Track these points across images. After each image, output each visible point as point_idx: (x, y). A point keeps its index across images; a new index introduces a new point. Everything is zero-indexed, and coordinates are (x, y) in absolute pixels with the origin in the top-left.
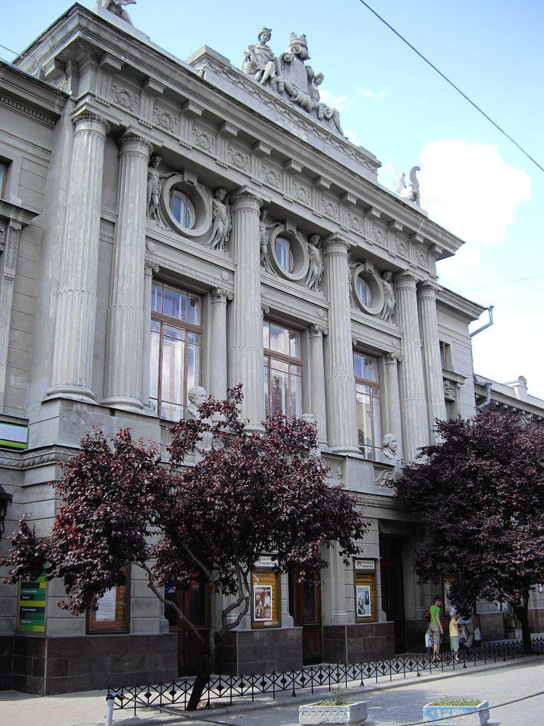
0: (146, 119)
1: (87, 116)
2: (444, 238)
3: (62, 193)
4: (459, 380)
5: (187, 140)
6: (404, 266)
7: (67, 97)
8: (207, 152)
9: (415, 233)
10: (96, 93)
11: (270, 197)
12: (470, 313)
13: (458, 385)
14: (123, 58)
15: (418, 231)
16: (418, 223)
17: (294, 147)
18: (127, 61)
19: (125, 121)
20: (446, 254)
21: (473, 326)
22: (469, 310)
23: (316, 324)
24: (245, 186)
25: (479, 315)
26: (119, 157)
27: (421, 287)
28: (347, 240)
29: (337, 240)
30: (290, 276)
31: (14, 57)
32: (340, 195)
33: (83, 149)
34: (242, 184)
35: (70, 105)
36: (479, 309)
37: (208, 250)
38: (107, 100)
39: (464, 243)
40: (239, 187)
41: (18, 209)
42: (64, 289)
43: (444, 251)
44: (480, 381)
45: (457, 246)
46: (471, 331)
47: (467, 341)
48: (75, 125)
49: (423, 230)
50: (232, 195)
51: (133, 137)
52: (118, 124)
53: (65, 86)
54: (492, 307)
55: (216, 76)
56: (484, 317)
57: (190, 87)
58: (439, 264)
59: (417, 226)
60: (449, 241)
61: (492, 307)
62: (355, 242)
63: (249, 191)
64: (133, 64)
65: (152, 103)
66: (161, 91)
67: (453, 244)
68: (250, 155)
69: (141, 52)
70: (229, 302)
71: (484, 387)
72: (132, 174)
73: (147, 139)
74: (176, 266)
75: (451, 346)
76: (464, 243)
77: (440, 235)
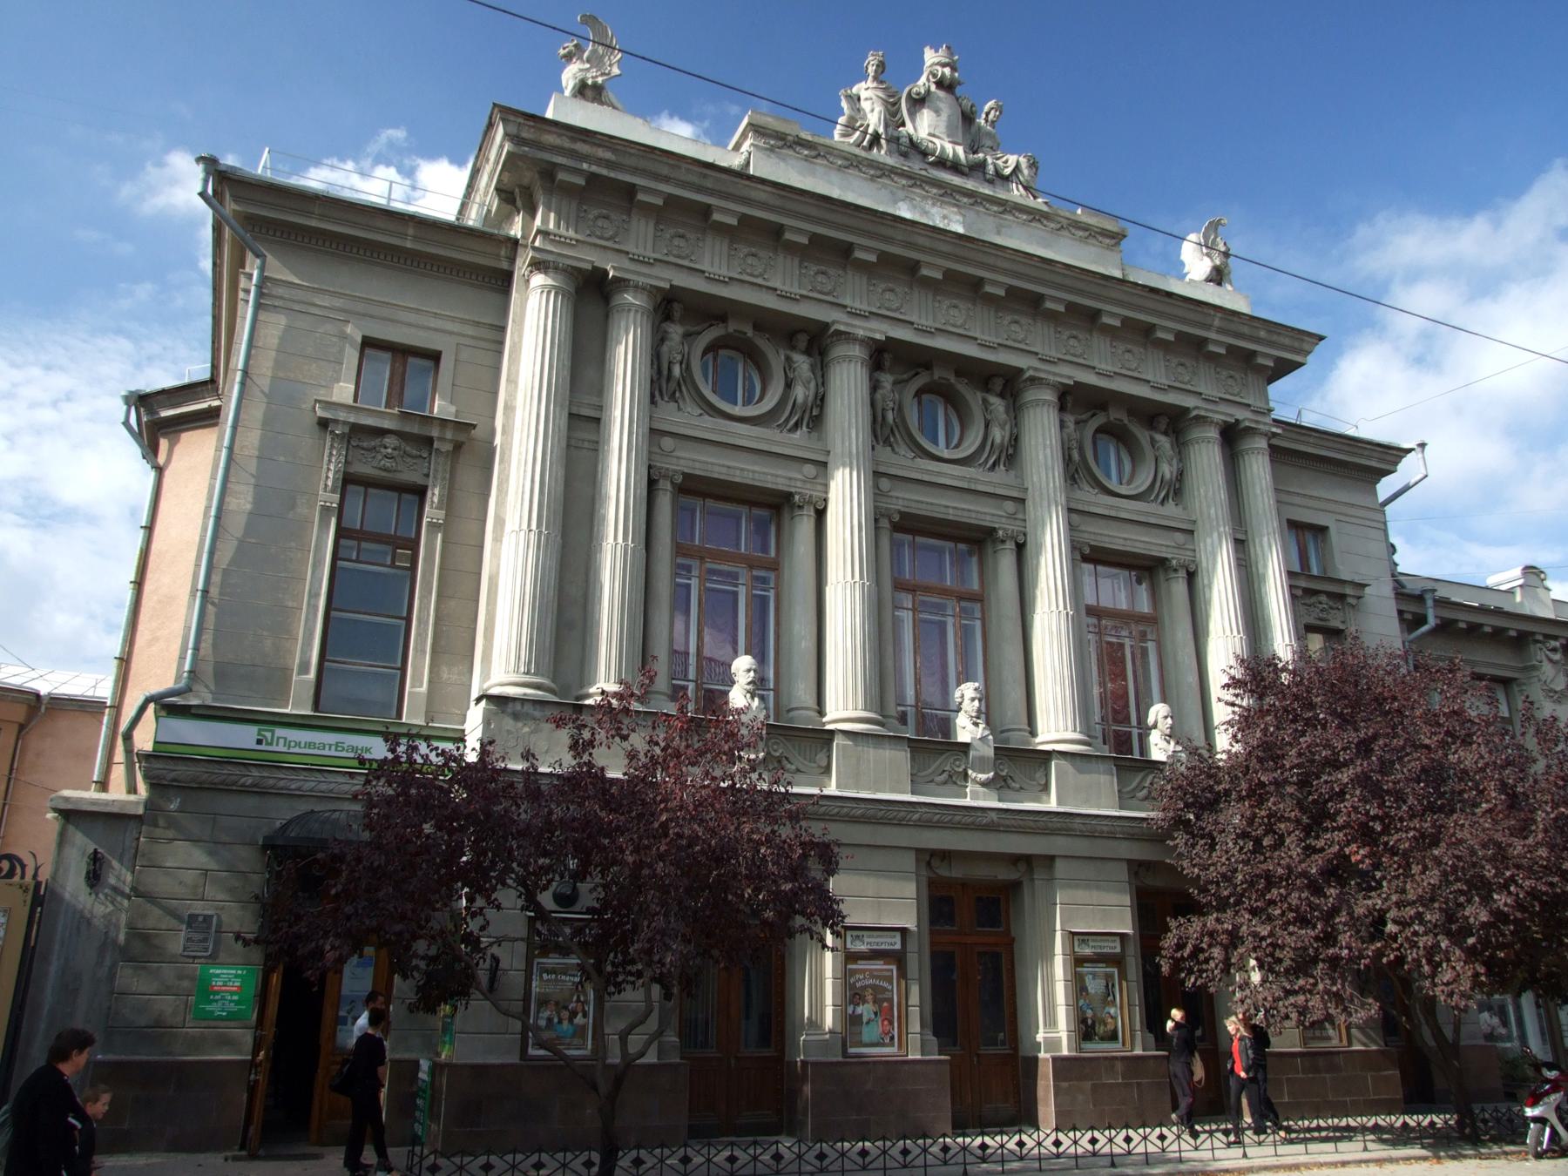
0: (638, 256)
2: (1275, 338)
4: (1348, 591)
5: (713, 269)
9: (1205, 341)
11: (880, 331)
12: (1374, 464)
13: (1350, 600)
14: (585, 166)
15: (1213, 335)
18: (594, 169)
20: (1284, 368)
21: (1385, 487)
22: (1369, 457)
24: (834, 322)
25: (1396, 463)
26: (607, 317)
27: (1232, 436)
28: (1051, 377)
29: (1033, 380)
30: (1123, 490)
34: (829, 320)
37: (785, 437)
39: (1321, 338)
40: (825, 326)
41: (444, 422)
43: (1278, 360)
44: (1413, 588)
45: (1306, 347)
46: (1381, 498)
47: (1378, 517)
49: (1221, 331)
50: (816, 341)
54: (1422, 445)
57: (709, 185)
58: (1277, 389)
59: (1208, 327)
60: (1287, 341)
61: (1422, 445)
63: (842, 328)
64: (604, 172)
67: (1296, 344)
68: (844, 268)
69: (614, 151)
71: (1420, 598)
73: (642, 280)
74: (717, 469)
75: (1333, 532)
76: (1321, 338)
77: (1262, 334)
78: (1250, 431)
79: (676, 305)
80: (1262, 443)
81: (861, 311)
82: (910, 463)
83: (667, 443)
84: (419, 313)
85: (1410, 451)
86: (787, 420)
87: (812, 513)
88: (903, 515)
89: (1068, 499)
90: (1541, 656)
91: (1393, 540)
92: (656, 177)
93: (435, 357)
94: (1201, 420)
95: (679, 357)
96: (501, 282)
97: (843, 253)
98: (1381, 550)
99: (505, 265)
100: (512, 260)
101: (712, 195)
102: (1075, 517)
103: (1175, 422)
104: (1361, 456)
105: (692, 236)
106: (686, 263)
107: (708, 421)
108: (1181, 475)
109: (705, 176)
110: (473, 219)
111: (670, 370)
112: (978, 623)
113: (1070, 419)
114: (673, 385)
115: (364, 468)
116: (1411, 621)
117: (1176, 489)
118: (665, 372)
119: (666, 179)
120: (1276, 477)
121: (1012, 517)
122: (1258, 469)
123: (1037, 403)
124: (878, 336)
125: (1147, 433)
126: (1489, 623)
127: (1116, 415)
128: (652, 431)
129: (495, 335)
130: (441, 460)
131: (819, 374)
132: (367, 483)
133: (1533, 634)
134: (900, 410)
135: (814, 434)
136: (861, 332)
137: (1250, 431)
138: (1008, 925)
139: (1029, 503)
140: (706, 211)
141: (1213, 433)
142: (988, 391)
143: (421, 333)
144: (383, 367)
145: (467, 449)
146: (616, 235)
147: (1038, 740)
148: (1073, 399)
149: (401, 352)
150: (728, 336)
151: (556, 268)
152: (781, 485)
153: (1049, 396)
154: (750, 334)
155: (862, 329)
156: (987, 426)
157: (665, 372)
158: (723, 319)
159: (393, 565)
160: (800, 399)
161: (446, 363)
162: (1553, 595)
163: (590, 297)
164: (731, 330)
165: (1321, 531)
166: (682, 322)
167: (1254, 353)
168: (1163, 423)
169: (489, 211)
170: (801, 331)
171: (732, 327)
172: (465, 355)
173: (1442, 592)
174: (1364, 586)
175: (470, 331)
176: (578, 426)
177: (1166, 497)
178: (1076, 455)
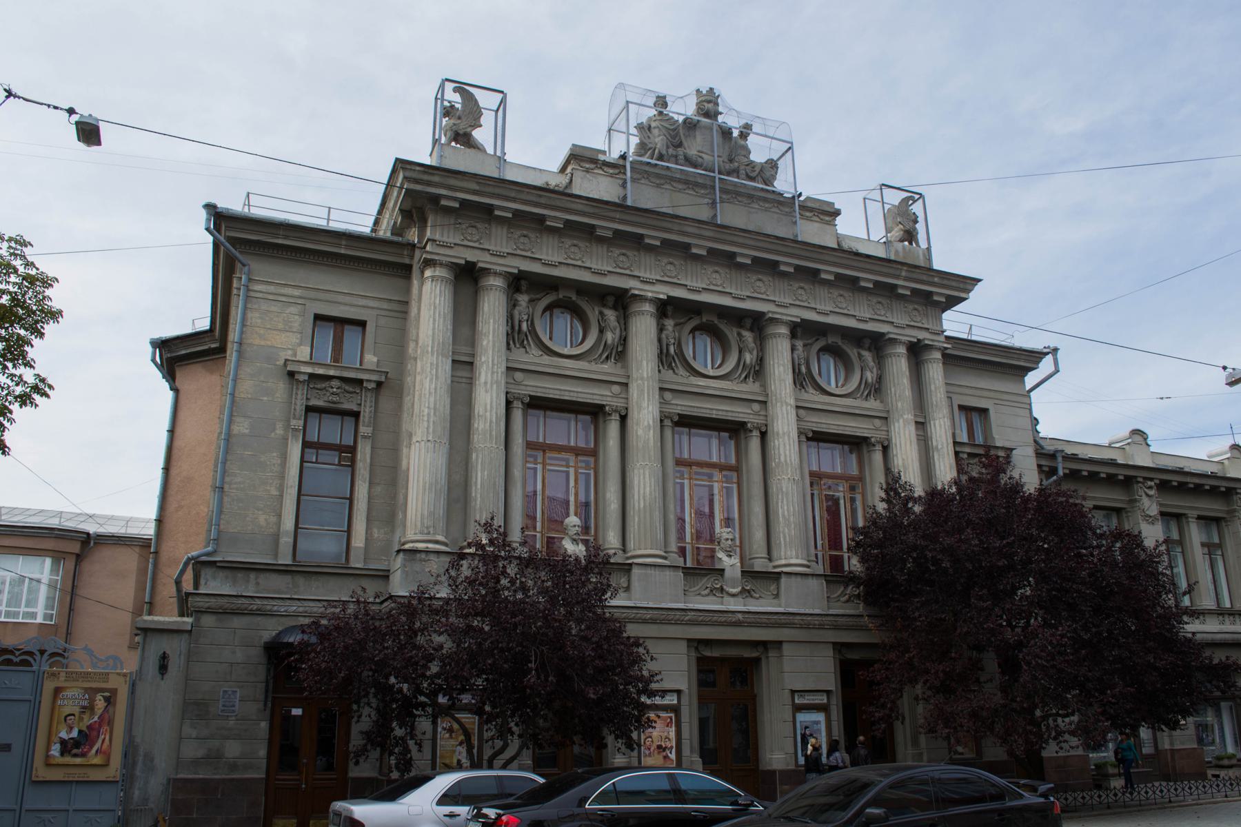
1: (428, 263)
3: (412, 345)
6: (883, 328)
7: (414, 246)
8: (579, 263)
10: (437, 237)
11: (663, 292)
12: (1022, 364)
16: (897, 273)
17: (690, 230)
19: (471, 256)
20: (953, 302)
21: (1031, 379)
22: (1019, 359)
25: (1038, 362)
29: (772, 319)
31: (370, 221)
32: (769, 268)
33: (431, 299)
35: (417, 253)
36: (1034, 357)
38: (451, 240)
42: (414, 440)
43: (948, 297)
44: (1050, 448)
47: (1025, 400)
48: (422, 273)
50: (621, 301)
51: (486, 272)
52: (463, 262)
53: (413, 236)
54: (1055, 350)
56: (1046, 365)
58: (947, 315)
65: (505, 230)
66: (510, 215)
72: (486, 309)
73: (498, 268)
75: (992, 413)
78: (929, 348)
79: (523, 282)
80: (938, 355)
81: (651, 280)
84: (350, 294)
85: (1047, 354)
89: (797, 400)
90: (1141, 492)
91: (1035, 414)
92: (507, 198)
93: (362, 324)
94: (893, 341)
96: (405, 271)
97: (636, 242)
98: (1027, 424)
99: (407, 261)
100: (412, 257)
102: (802, 412)
103: (877, 343)
104: (1012, 358)
105: (532, 235)
108: (880, 379)
109: (540, 196)
110: (384, 232)
112: (735, 486)
113: (799, 344)
114: (523, 336)
115: (313, 402)
116: (1047, 471)
119: (514, 200)
120: (946, 374)
122: (935, 372)
124: (661, 296)
125: (855, 351)
126: (1104, 471)
127: (831, 340)
128: (508, 368)
129: (402, 310)
130: (369, 394)
132: (320, 411)
133: (1136, 477)
134: (679, 345)
135: (619, 365)
136: (650, 294)
138: (752, 685)
141: (902, 350)
142: (742, 327)
143: (353, 309)
144: (328, 334)
145: (388, 386)
148: (801, 330)
149: (340, 323)
151: (441, 264)
153: (784, 330)
159: (339, 464)
161: (370, 328)
162: (1152, 449)
163: (467, 277)
165: (984, 412)
167: (931, 293)
168: (867, 342)
169: (395, 223)
172: (382, 321)
173: (1070, 450)
174: (1012, 450)
175: (385, 305)
176: (464, 365)
177: (869, 394)
178: (803, 369)
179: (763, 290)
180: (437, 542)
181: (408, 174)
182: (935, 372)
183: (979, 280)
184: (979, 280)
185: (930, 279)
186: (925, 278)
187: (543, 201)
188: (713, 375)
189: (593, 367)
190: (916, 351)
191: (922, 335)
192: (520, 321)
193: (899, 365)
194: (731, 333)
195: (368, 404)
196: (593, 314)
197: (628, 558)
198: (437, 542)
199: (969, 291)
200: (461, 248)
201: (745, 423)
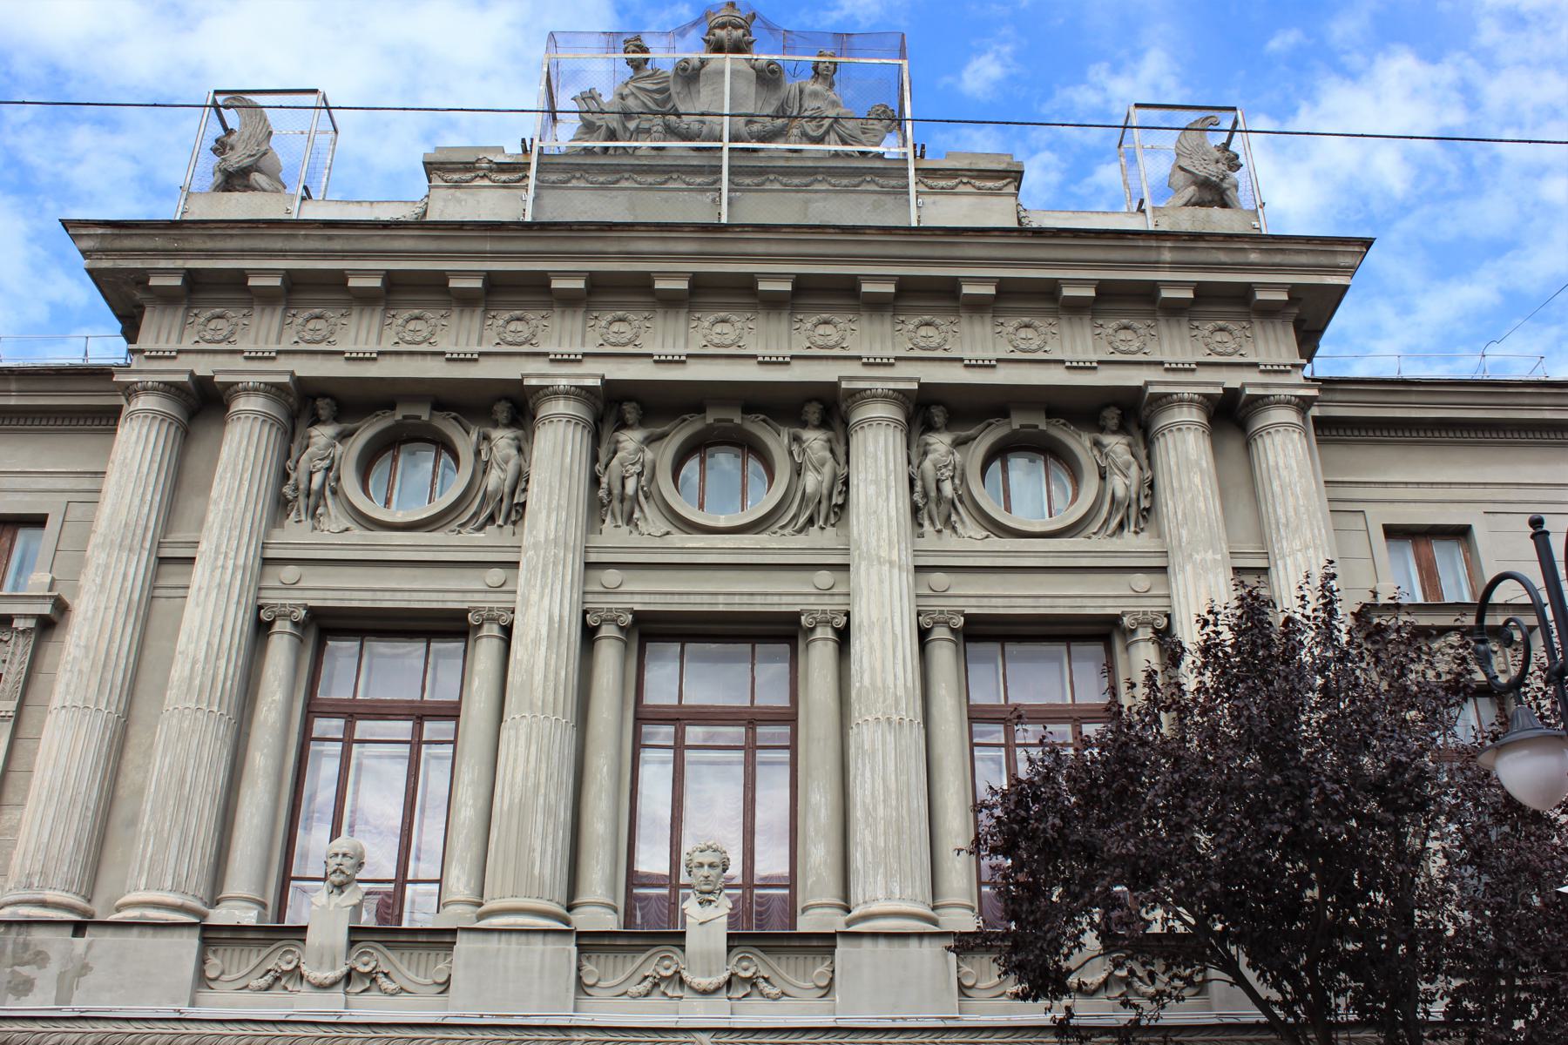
9: (1154, 286)
11: (592, 374)
23: (1124, 614)
28: (879, 385)
49: (1176, 266)
55: (458, 193)
59: (1155, 265)
62: (910, 380)
63: (534, 382)
70: (843, 637)
81: (566, 352)
82: (979, 546)
83: (939, 579)
86: (1106, 521)
87: (830, 634)
88: (640, 618)
95: (948, 473)
101: (344, 258)
106: (323, 347)
107: (680, 539)
111: (939, 489)
117: (1143, 510)
118: (933, 494)
121: (498, 588)
123: (1179, 427)
125: (1087, 439)
130: (21, 641)
131: (1142, 453)
136: (563, 382)
137: (1260, 403)
139: (1170, 570)
140: (339, 279)
146: (232, 333)
147: (855, 912)
148: (925, 410)
150: (1015, 432)
151: (145, 389)
152: (453, 602)
154: (1043, 426)
155: (563, 378)
156: (1103, 477)
157: (933, 494)
158: (699, 409)
160: (1120, 493)
164: (1016, 426)
166: (948, 427)
167: (1249, 288)
170: (1107, 406)
171: (1017, 422)
179: (1231, 346)
180: (43, 904)
181: (88, 244)
182: (1285, 451)
183: (1367, 243)
184: (1367, 243)
185: (1239, 258)
186: (1222, 257)
187: (336, 245)
188: (716, 529)
189: (454, 539)
190: (1231, 416)
191: (1233, 379)
192: (938, 481)
193: (1186, 448)
194: (1080, 444)
195: (18, 657)
196: (465, 444)
197: (481, 917)
198: (43, 904)
199: (1351, 270)
200: (192, 357)
201: (796, 616)
